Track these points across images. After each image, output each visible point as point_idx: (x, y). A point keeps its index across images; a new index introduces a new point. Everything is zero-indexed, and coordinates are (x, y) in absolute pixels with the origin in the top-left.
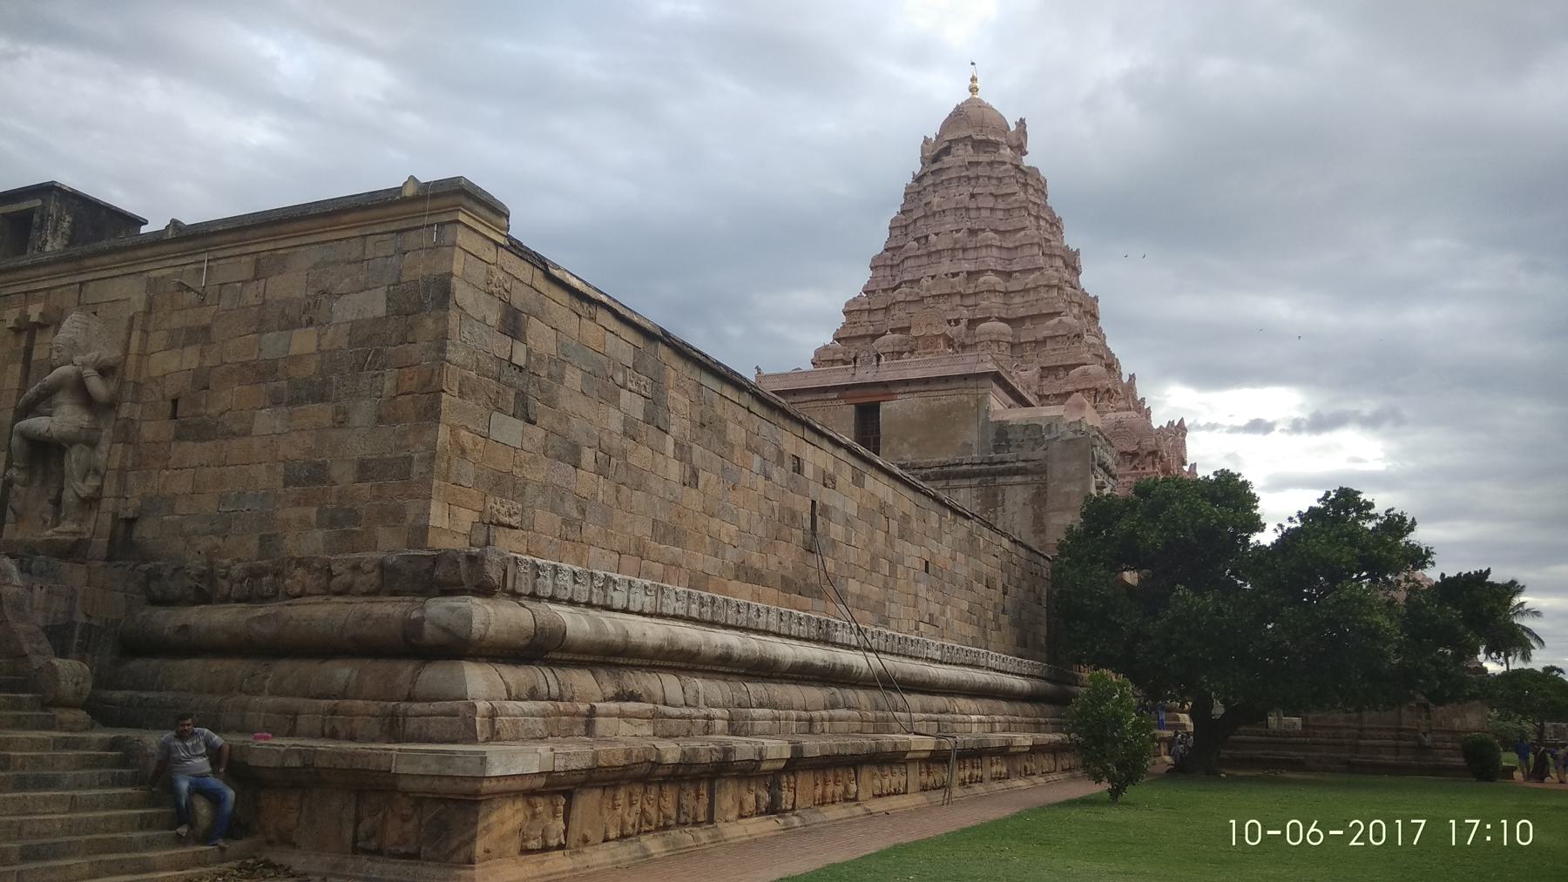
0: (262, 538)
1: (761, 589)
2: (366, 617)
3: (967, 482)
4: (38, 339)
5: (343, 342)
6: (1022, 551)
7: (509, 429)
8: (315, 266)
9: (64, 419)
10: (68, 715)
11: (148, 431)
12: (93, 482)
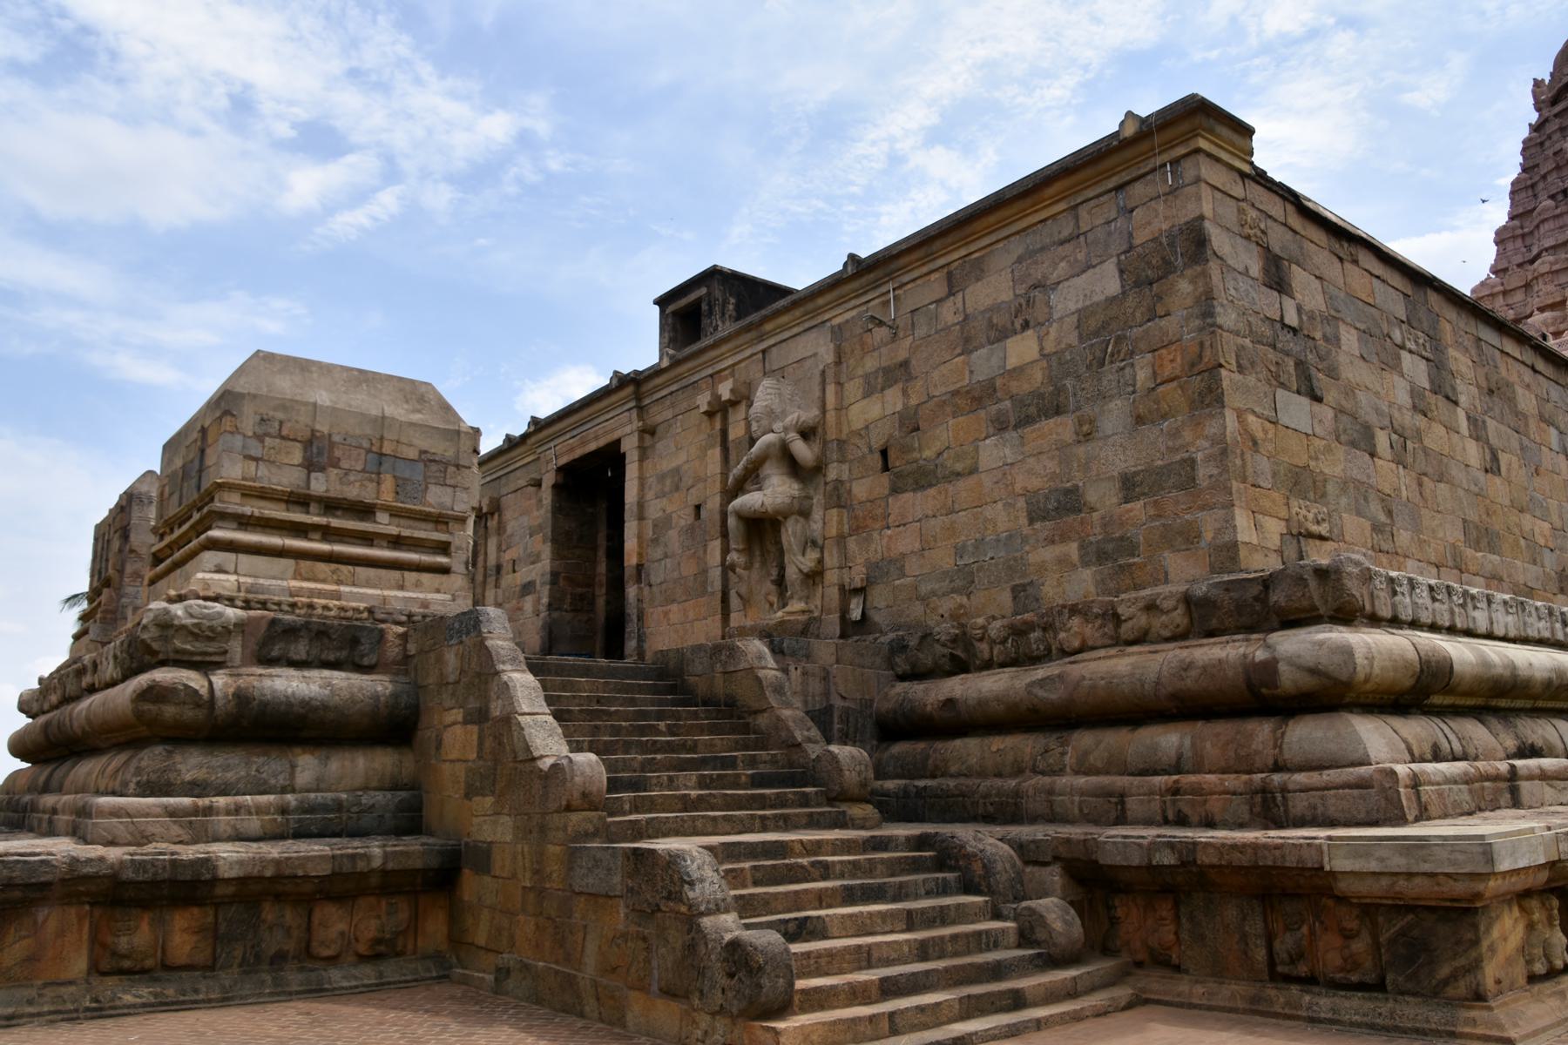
0: (1017, 591)
2: (1187, 667)
4: (731, 418)
5: (1073, 338)
7: (1296, 410)
8: (1020, 260)
9: (775, 491)
10: (856, 811)
11: (860, 490)
12: (813, 555)
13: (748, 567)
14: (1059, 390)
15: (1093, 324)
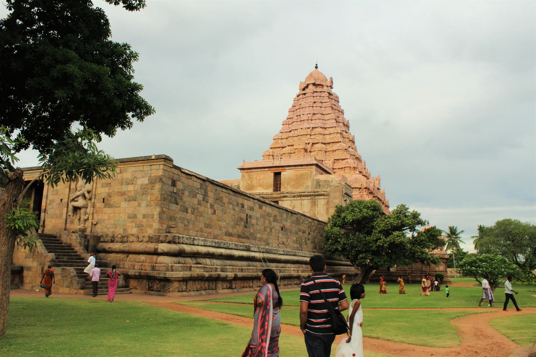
0: (124, 230)
1: (232, 238)
3: (306, 198)
6: (316, 222)
9: (80, 202)
12: (87, 216)
13: (73, 216)
14: (136, 197)
15: (143, 187)
